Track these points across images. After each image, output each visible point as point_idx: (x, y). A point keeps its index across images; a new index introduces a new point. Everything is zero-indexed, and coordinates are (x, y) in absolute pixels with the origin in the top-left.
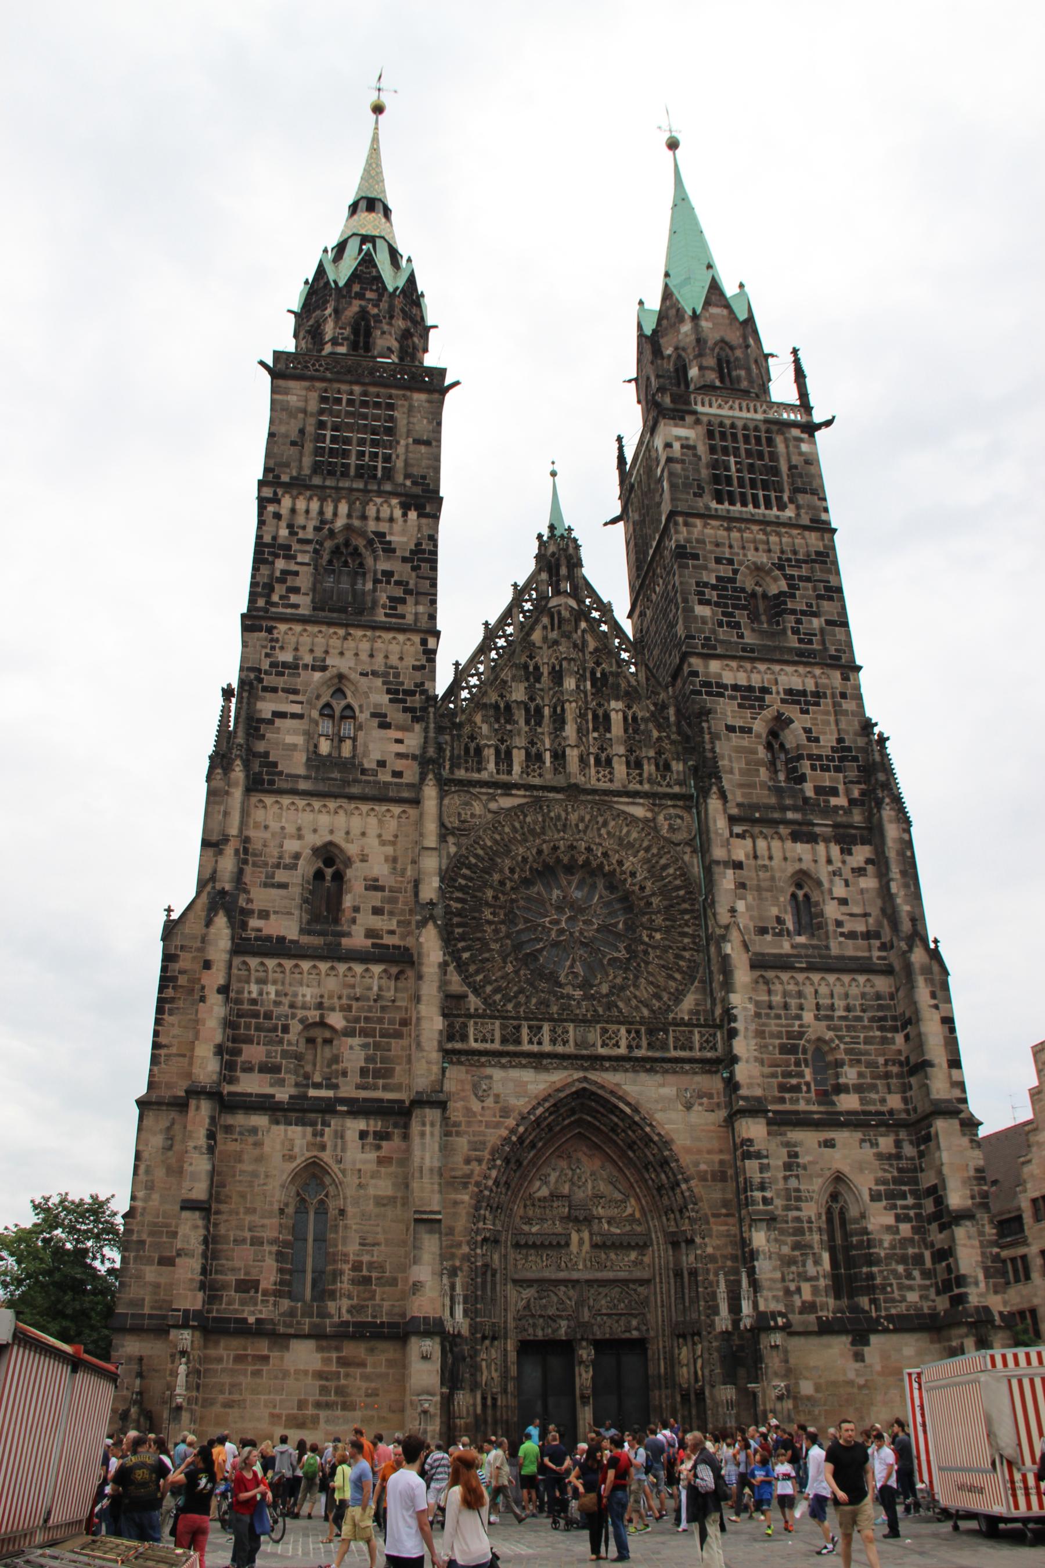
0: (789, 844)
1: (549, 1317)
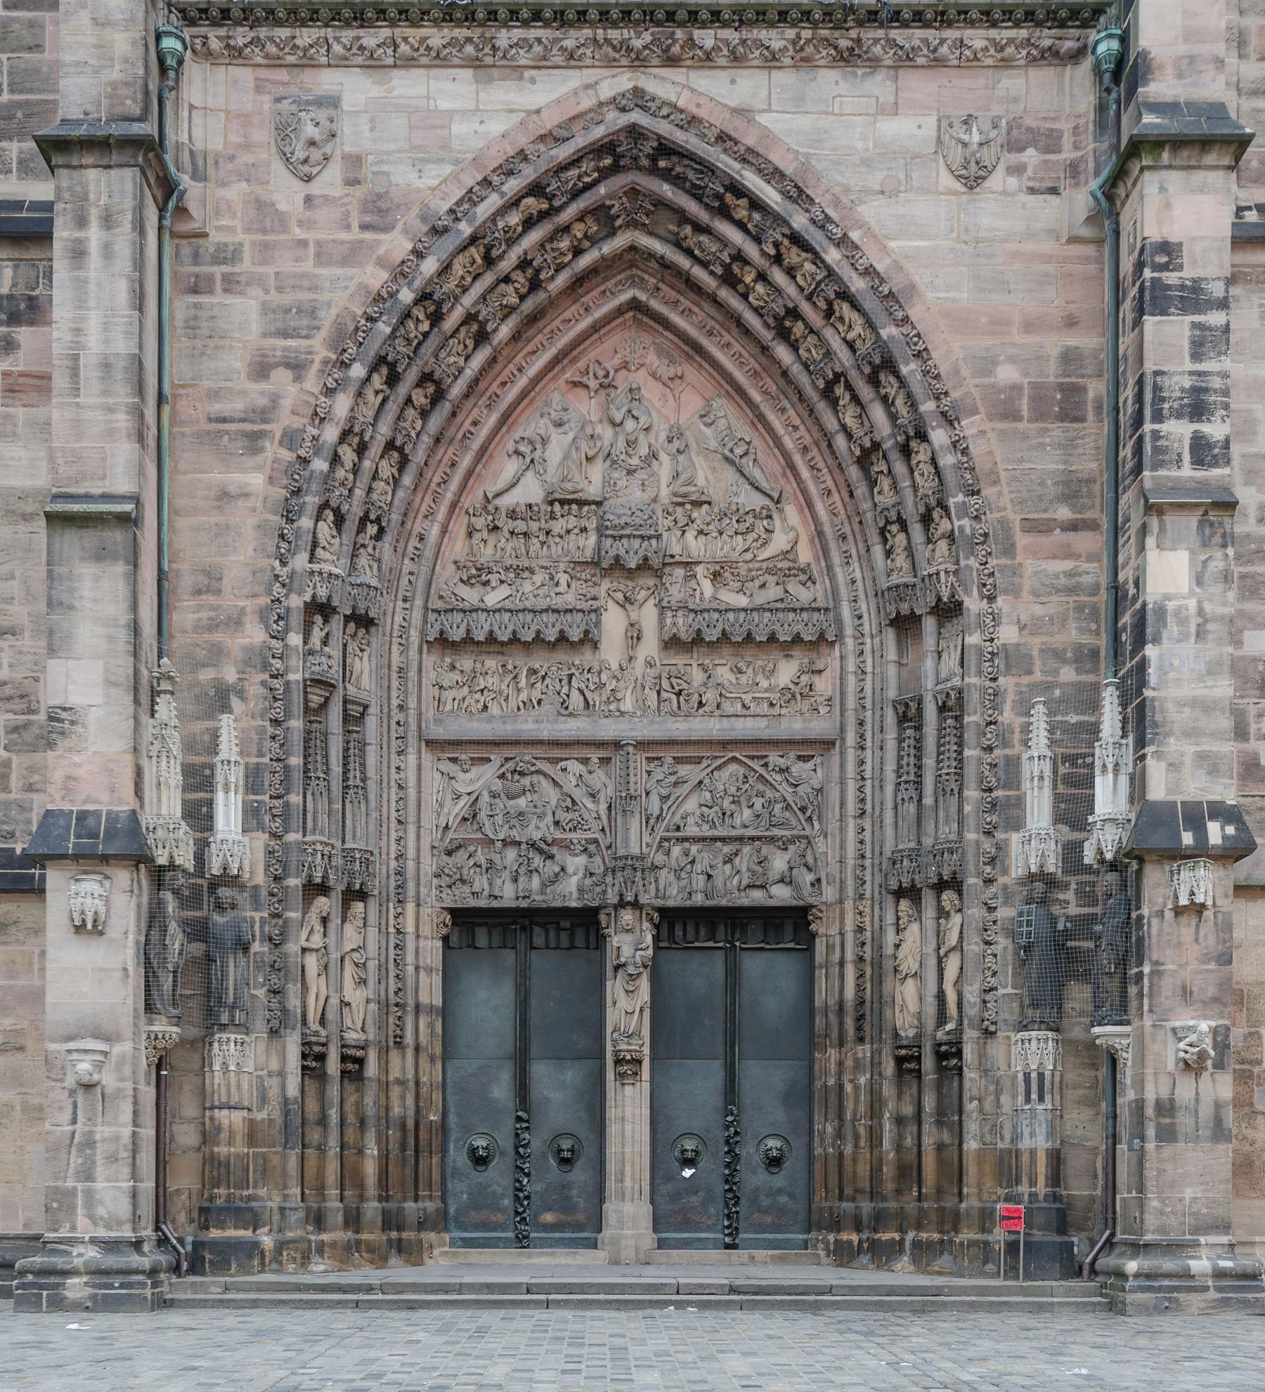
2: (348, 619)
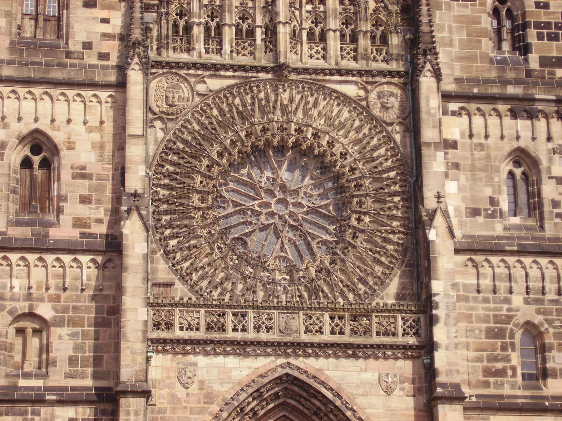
0: (508, 121)
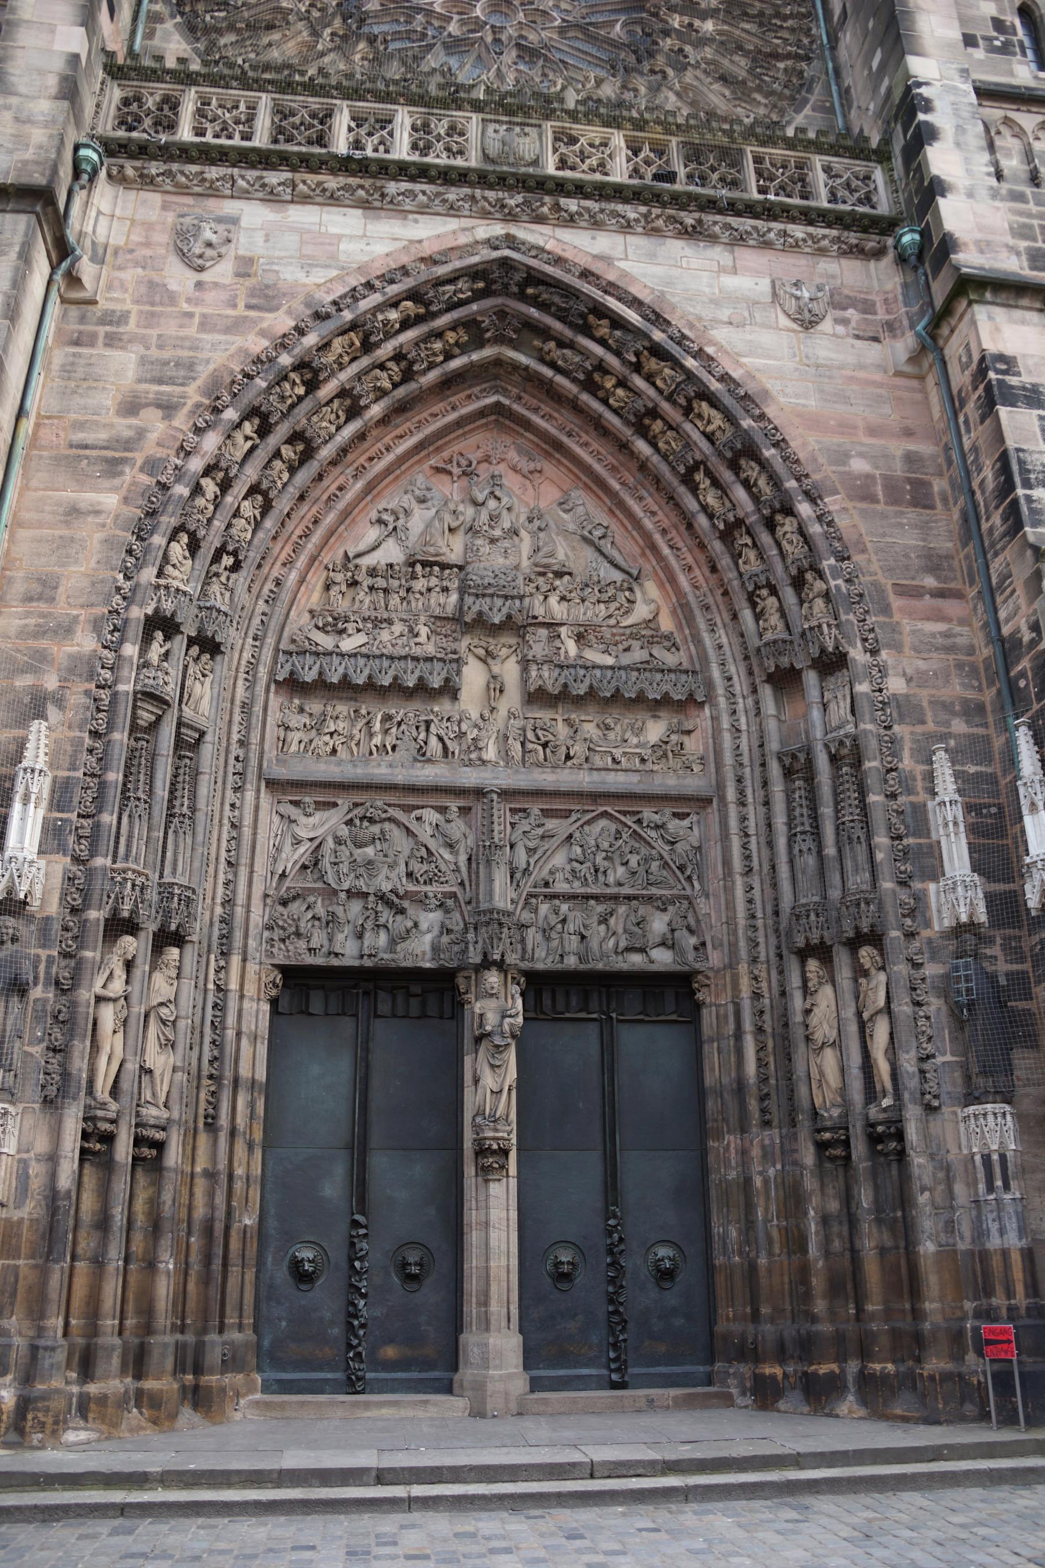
1: (381, 897)
2: (191, 642)
